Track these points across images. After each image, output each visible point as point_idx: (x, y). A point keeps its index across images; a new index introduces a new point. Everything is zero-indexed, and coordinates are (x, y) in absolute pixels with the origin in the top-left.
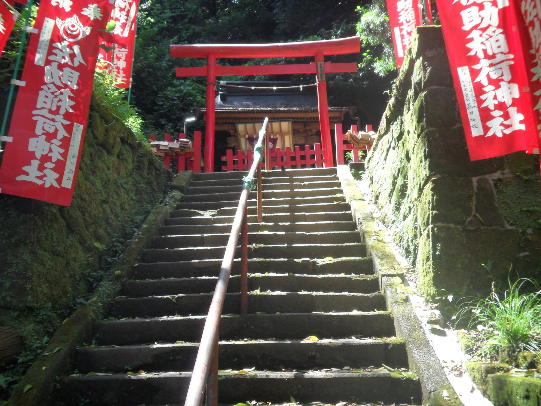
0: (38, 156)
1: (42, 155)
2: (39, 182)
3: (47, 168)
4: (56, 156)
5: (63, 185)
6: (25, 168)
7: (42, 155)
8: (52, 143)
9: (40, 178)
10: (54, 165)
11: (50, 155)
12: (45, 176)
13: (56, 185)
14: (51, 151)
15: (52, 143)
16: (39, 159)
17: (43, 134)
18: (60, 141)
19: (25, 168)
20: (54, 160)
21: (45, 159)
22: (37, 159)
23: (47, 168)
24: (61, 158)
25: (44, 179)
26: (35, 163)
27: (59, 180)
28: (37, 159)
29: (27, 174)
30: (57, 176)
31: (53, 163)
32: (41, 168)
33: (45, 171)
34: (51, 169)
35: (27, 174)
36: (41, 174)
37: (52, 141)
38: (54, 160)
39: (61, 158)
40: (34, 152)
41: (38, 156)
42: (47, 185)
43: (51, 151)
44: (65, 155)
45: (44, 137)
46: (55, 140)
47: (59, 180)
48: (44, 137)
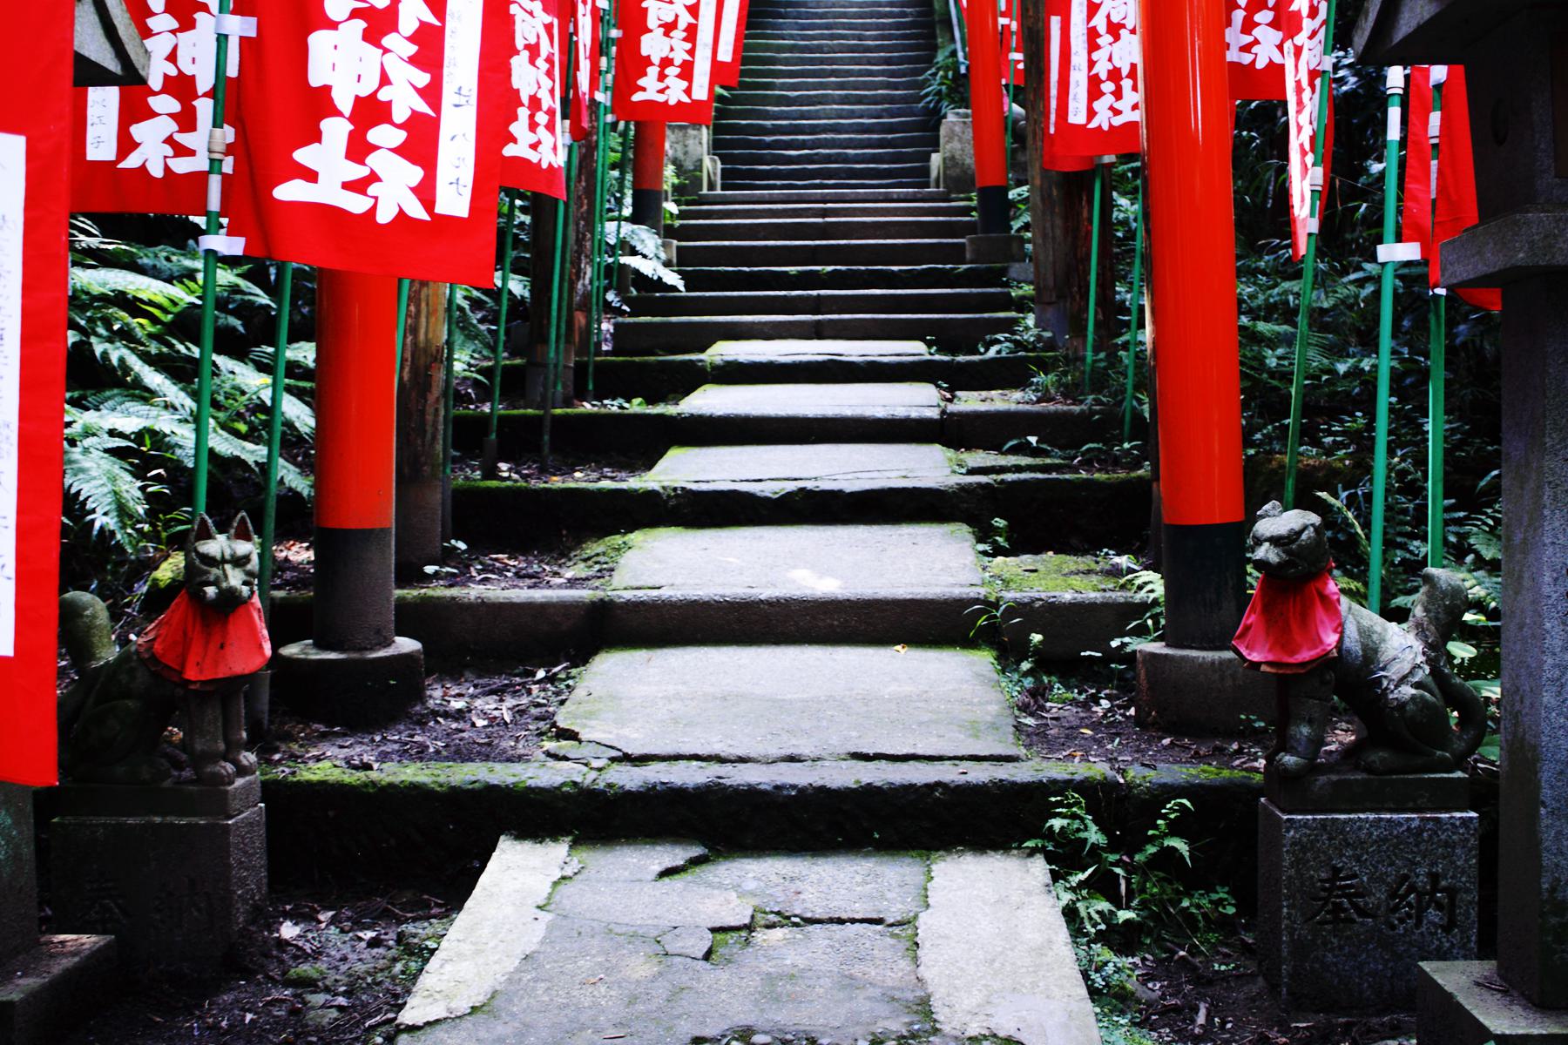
0: (344, 103)
1: (357, 97)
2: (356, 204)
3: (376, 148)
4: (404, 101)
5: (439, 209)
6: (303, 156)
7: (357, 97)
8: (386, 51)
9: (357, 187)
10: (400, 137)
11: (383, 96)
12: (373, 178)
13: (417, 211)
14: (385, 80)
15: (386, 51)
16: (347, 113)
17: (355, 14)
18: (411, 39)
19: (303, 156)
20: (400, 115)
21: (370, 111)
22: (339, 114)
23: (376, 148)
24: (423, 108)
25: (373, 189)
26: (336, 130)
27: (425, 192)
28: (339, 114)
29: (311, 176)
30: (416, 174)
31: (399, 126)
32: (358, 149)
33: (372, 160)
34: (394, 150)
35: (311, 176)
36: (357, 172)
37: (387, 41)
38: (400, 115)
39: (423, 108)
40: (327, 89)
41: (344, 103)
42: (384, 216)
43: (385, 80)
44: (432, 93)
45: (360, 25)
46: (394, 35)
47: (425, 192)
48: (360, 25)
